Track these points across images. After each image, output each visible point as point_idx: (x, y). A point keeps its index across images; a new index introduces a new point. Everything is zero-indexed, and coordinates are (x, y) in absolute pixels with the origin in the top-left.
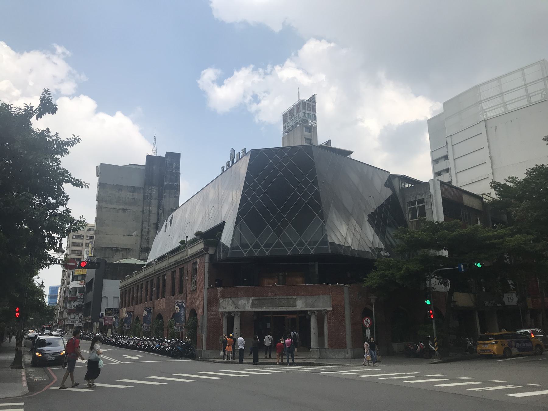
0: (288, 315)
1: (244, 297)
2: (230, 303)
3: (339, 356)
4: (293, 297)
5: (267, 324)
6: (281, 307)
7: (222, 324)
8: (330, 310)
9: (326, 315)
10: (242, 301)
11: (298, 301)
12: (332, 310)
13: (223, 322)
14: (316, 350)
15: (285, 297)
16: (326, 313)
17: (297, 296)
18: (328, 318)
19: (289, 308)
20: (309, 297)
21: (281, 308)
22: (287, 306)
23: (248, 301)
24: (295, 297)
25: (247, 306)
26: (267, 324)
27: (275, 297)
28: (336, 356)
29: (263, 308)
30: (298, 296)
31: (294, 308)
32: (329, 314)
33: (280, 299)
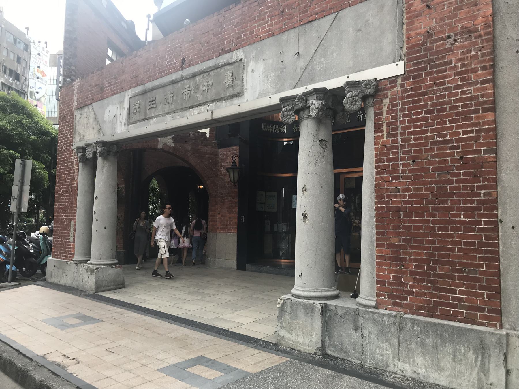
0: (345, 170)
1: (114, 94)
2: (92, 120)
3: (441, 369)
4: (234, 53)
5: (293, 196)
6: (197, 106)
7: (75, 185)
8: (392, 80)
9: (371, 113)
10: (110, 108)
11: (252, 65)
12: (405, 77)
13: (78, 178)
14: (305, 306)
15: (211, 63)
16: (373, 96)
17: (246, 45)
18: (378, 128)
19: (218, 108)
20: (292, 33)
21: (196, 110)
22: (212, 102)
23: (122, 102)
24: (239, 54)
25: (118, 121)
26: (293, 196)
27: (180, 73)
28: (419, 360)
29: (152, 121)
30: (250, 44)
31: (236, 101)
32: (386, 101)
33: (194, 76)
